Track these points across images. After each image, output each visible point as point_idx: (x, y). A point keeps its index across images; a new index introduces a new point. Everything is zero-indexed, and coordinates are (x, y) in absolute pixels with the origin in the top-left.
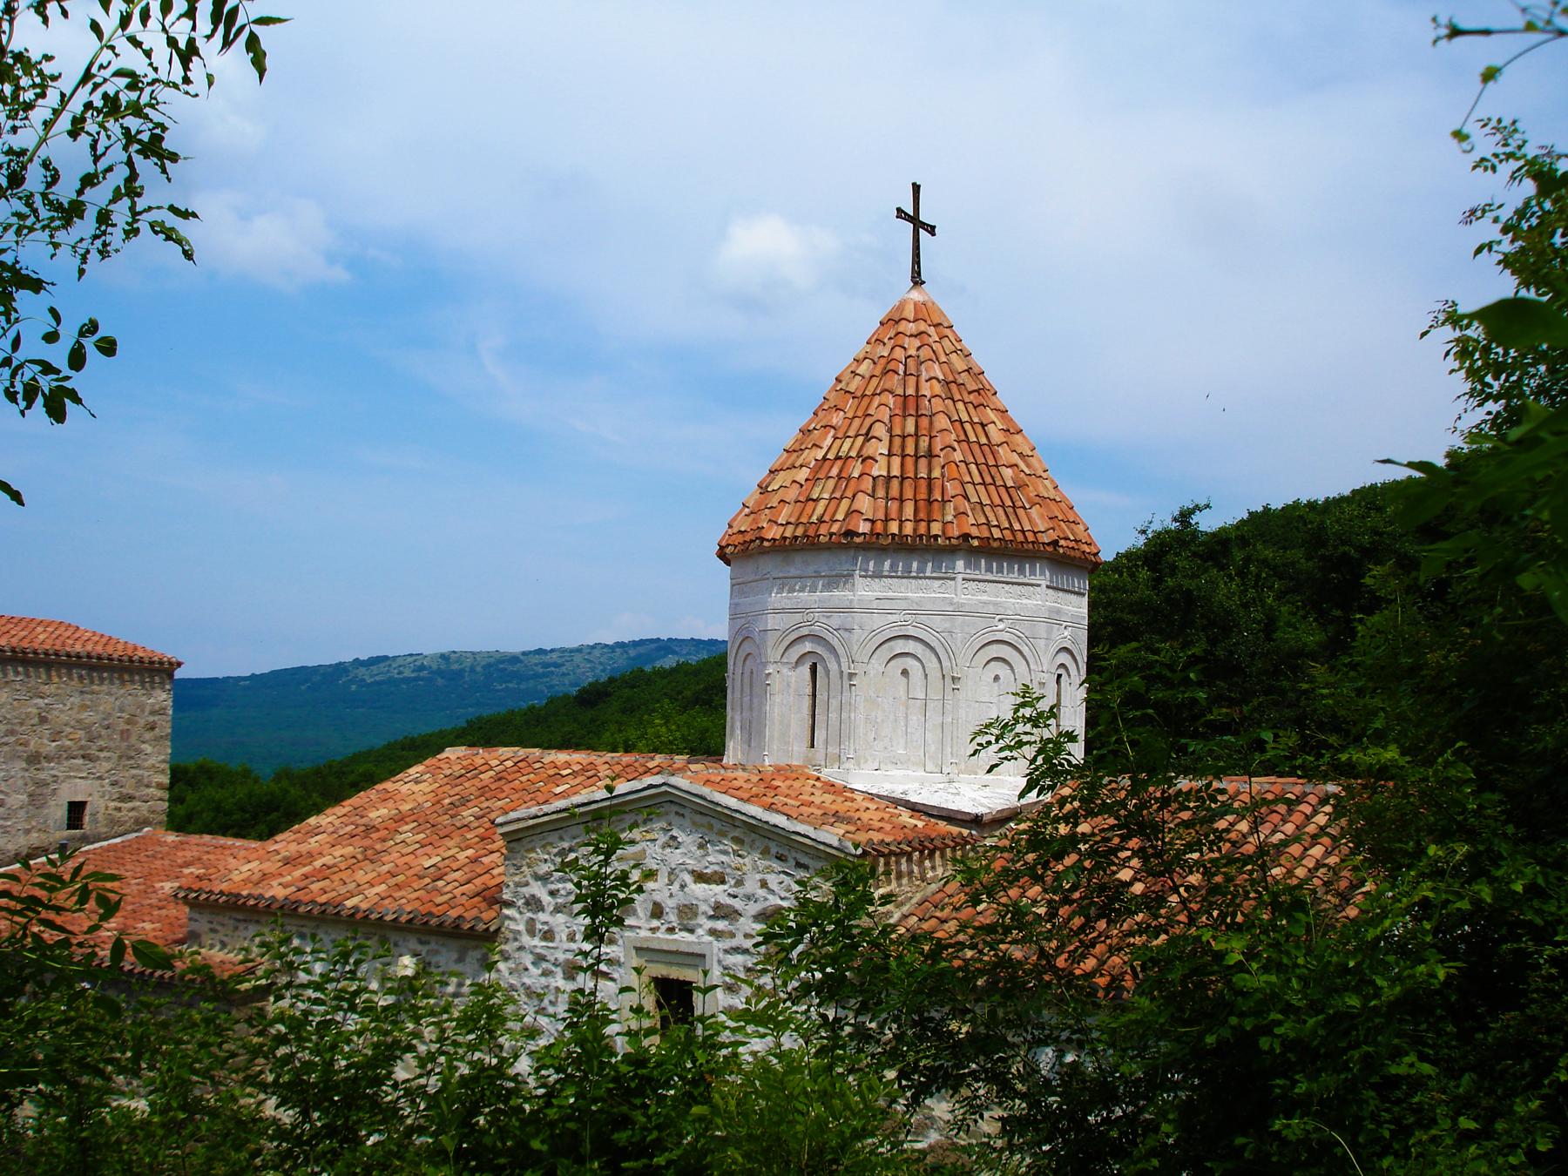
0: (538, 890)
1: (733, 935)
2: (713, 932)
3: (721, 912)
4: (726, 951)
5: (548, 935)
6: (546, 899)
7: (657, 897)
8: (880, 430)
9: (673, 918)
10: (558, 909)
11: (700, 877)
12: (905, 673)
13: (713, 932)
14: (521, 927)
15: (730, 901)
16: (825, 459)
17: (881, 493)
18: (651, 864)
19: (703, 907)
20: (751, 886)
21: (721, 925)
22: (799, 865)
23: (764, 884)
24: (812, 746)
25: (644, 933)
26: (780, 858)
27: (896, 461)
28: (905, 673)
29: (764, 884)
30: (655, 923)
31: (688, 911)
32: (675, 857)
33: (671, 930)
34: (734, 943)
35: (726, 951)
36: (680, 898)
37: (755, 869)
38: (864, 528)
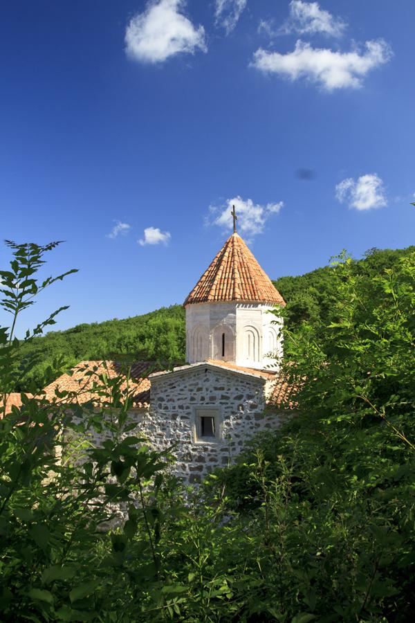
0: (162, 395)
1: (227, 403)
2: (221, 403)
3: (223, 397)
4: (226, 408)
5: (166, 408)
6: (165, 398)
7: (202, 395)
8: (236, 271)
9: (207, 400)
10: (168, 401)
11: (216, 389)
12: (249, 336)
13: (221, 403)
14: (157, 406)
15: (227, 395)
16: (221, 278)
17: (241, 288)
18: (200, 386)
19: (217, 397)
20: (233, 389)
21: (224, 401)
22: (247, 384)
23: (237, 389)
24: (223, 355)
25: (198, 405)
26: (241, 382)
27: (242, 279)
28: (249, 336)
29: (237, 389)
30: (202, 402)
31: (213, 398)
32: (207, 384)
33: (208, 403)
34: (228, 405)
35: (226, 408)
36: (210, 395)
37: (234, 385)
38: (239, 297)
